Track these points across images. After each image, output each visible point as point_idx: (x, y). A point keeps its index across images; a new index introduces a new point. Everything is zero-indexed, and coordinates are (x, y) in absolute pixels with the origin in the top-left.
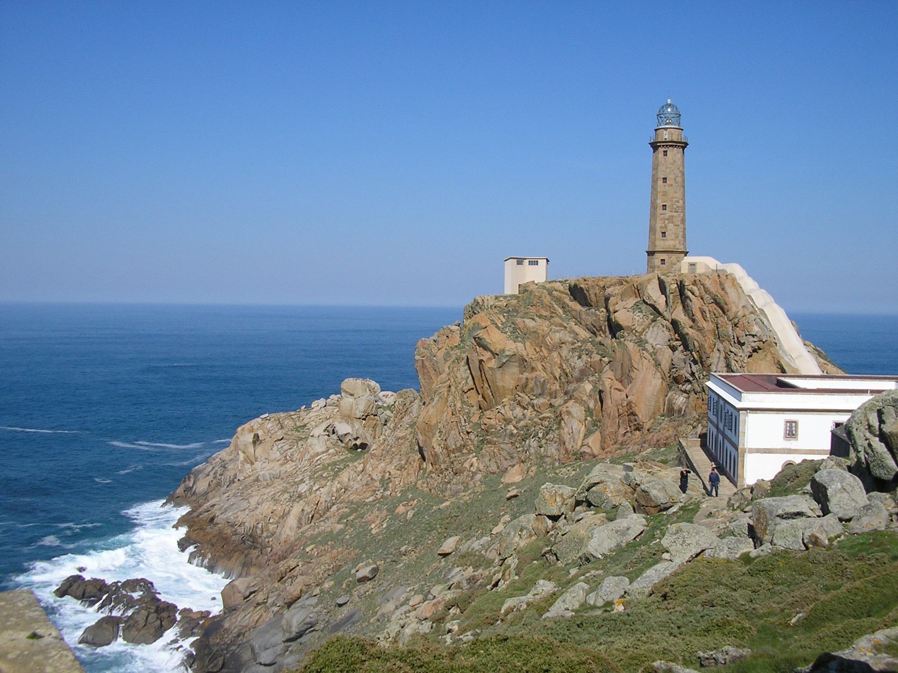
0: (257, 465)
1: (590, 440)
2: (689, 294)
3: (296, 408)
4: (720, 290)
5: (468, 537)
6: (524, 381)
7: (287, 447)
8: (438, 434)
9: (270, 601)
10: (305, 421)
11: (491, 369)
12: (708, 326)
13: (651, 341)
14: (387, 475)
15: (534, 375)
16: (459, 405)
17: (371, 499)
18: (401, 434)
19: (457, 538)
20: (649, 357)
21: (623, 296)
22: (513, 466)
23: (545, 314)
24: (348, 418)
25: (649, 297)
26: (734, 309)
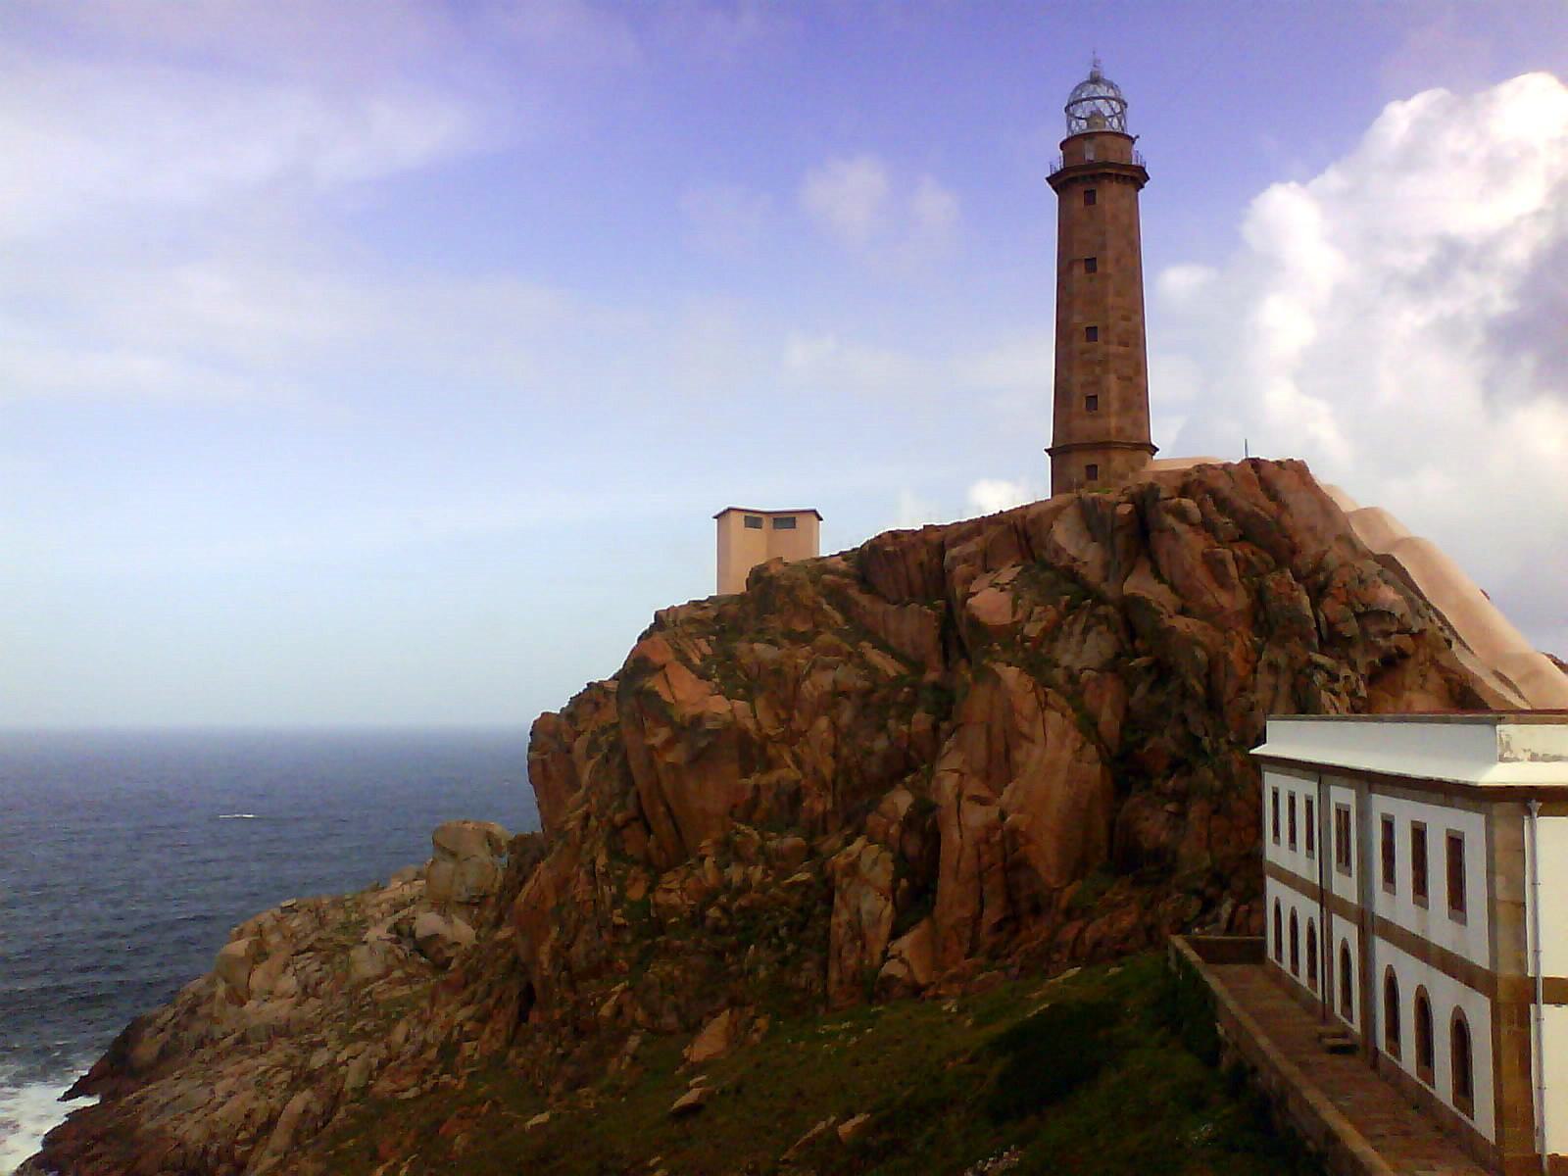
0: (251, 1005)
1: (905, 943)
2: (1170, 520)
4: (1264, 500)
6: (749, 795)
8: (555, 931)
11: (674, 766)
12: (1234, 601)
13: (1066, 659)
15: (773, 777)
16: (602, 861)
20: (1063, 702)
21: (987, 563)
22: (714, 1015)
25: (1059, 551)
26: (1312, 549)
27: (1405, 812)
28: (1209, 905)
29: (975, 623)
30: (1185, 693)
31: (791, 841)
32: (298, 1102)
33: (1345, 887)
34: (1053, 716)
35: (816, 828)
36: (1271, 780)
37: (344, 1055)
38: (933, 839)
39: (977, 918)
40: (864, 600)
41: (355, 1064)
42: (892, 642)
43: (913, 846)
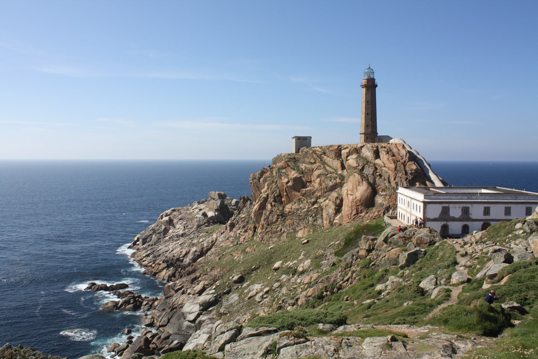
1: (338, 217)
3: (185, 204)
5: (286, 262)
7: (185, 223)
9: (188, 292)
10: (191, 211)
11: (290, 186)
12: (393, 166)
14: (238, 235)
17: (232, 245)
18: (243, 216)
19: (281, 262)
22: (301, 229)
23: (313, 161)
24: (210, 209)
27: (416, 202)
28: (388, 211)
29: (349, 166)
30: (385, 180)
31: (313, 200)
32: (194, 249)
33: (409, 210)
34: (364, 182)
35: (318, 198)
36: (399, 195)
37: (201, 240)
38: (342, 200)
39: (351, 213)
40: (325, 157)
41: (205, 242)
42: (331, 165)
43: (338, 201)
